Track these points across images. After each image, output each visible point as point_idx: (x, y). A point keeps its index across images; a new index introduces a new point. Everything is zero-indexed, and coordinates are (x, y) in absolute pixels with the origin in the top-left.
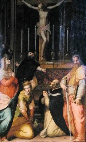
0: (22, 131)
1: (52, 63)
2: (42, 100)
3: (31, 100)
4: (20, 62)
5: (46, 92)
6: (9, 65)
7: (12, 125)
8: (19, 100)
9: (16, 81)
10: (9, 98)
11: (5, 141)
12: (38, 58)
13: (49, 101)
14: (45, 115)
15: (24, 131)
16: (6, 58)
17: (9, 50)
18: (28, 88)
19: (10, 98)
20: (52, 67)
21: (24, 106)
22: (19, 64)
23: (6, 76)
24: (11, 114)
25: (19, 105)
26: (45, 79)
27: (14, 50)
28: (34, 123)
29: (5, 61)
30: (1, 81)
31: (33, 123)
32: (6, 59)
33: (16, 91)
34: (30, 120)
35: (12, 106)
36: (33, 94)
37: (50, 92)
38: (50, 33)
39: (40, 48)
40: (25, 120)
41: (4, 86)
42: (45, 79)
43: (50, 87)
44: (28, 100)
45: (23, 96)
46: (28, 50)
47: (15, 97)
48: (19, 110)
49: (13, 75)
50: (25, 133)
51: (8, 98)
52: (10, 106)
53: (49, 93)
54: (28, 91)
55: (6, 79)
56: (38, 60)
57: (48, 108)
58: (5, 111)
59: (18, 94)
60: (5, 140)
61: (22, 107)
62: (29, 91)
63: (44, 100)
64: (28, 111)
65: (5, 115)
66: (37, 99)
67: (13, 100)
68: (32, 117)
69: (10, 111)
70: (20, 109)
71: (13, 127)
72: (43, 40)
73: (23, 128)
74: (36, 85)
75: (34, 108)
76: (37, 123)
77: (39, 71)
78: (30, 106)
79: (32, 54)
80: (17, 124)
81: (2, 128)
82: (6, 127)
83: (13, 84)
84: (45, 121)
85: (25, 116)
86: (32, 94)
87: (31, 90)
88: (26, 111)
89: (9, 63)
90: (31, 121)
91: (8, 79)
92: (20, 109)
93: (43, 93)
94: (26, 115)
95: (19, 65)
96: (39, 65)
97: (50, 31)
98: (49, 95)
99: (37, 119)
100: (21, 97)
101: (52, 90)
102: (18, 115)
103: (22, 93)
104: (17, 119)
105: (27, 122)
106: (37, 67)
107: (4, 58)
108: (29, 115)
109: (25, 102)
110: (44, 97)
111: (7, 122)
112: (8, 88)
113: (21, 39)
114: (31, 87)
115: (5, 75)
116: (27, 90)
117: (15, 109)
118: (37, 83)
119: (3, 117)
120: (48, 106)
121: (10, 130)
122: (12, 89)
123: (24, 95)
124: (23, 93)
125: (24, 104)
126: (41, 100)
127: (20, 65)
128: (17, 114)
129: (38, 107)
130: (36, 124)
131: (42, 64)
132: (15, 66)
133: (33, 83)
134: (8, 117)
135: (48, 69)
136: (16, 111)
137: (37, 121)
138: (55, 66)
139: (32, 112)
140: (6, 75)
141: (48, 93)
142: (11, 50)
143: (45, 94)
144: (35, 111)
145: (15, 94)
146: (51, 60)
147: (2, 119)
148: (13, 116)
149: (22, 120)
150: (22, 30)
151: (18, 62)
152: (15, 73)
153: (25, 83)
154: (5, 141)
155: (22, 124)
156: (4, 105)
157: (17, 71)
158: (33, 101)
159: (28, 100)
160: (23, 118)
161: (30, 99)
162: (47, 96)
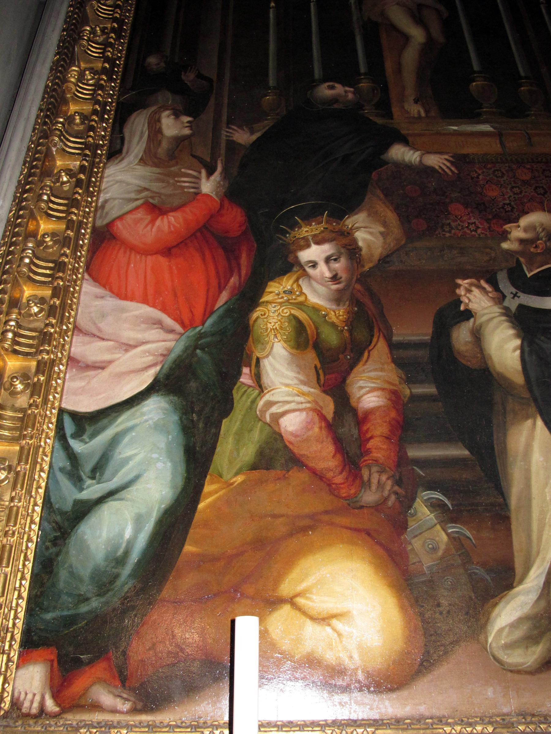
0: (291, 601)
1: (486, 128)
2: (461, 336)
3: (361, 335)
4: (267, 124)
5: (483, 283)
6: (179, 141)
7: (189, 548)
8: (258, 341)
9: (234, 218)
10: (168, 321)
11: (96, 707)
12: (384, 107)
13: (518, 342)
14: (504, 451)
15: (318, 602)
16: (165, 108)
17: (189, 77)
18: (328, 260)
19: (178, 328)
20: (493, 147)
21: (303, 383)
22: (258, 135)
23: (159, 194)
24: (179, 455)
25: (258, 377)
26: (457, 209)
27: (220, 76)
28: (412, 524)
29: (159, 121)
30: (119, 224)
31: (399, 522)
32: (167, 113)
33: (234, 280)
34: (369, 497)
35: (193, 385)
36: (372, 295)
37: (514, 285)
38: (445, 14)
39: (389, 66)
40: (317, 502)
41: (133, 248)
42: (457, 209)
43: (509, 253)
44: (331, 338)
45: (287, 312)
46: (317, 72)
47: (221, 319)
48: (253, 416)
49: (208, 186)
50: (324, 619)
51: (159, 323)
52: (170, 382)
53: (507, 288)
54: (335, 278)
55: (155, 209)
56: (389, 115)
57: (527, 395)
58: (123, 421)
59: (250, 297)
60: (106, 697)
61: (283, 389)
62: (343, 275)
63: (477, 336)
64: (342, 420)
65: (124, 450)
66: (414, 329)
67: (201, 336)
68: (380, 472)
69: (175, 418)
70: (270, 404)
71: (202, 561)
72: (407, 38)
73: (294, 574)
74: (389, 239)
75: (394, 396)
76: (443, 523)
77: (409, 167)
78: (361, 383)
79: (339, 89)
80: (238, 532)
81: (85, 573)
82: (120, 561)
83: (205, 236)
84: (513, 502)
85: (320, 465)
86: (366, 300)
87: (350, 270)
88: (323, 417)
89: (187, 132)
90: (378, 507)
91: (175, 209)
92: (270, 404)
93: (461, 292)
94: (323, 455)
95: (254, 137)
96: (404, 141)
97: (442, 8)
98: (513, 304)
99: (430, 487)
100: (272, 314)
101: (529, 276)
102: (249, 452)
103: (275, 289)
104: (243, 489)
105: (338, 520)
106: (387, 146)
107: (153, 109)
108: (352, 456)
109: (311, 357)
110: (468, 314)
111: (139, 520)
112: (162, 260)
113: (267, 32)
114: (352, 251)
115: (146, 189)
116: (323, 270)
117: (225, 406)
118: (397, 231)
119: (98, 470)
120: (519, 379)
121: (167, 592)
122: (196, 273)
123: (301, 305)
124: (290, 292)
125: (300, 368)
126: (448, 336)
127: (258, 139)
128: (234, 449)
129: (430, 389)
130: (430, 532)
131: (420, 135)
132: (223, 145)
133: (368, 232)
134: (150, 475)
135: (465, 156)
136: (230, 426)
137: (435, 506)
138: (513, 145)
139: (378, 429)
140: (156, 186)
141: (496, 288)
142: (200, 76)
143: (477, 299)
144: (407, 423)
145: (224, 297)
146: (479, 114)
147: (92, 490)
148: (197, 460)
149: (288, 496)
150: (272, 4)
151: (248, 124)
152: (226, 173)
153: (305, 231)
154: (96, 707)
155: (291, 535)
156: (120, 376)
157: (243, 166)
158: (380, 349)
159: (331, 338)
160: (299, 477)
161: (350, 331)
162: (497, 310)
